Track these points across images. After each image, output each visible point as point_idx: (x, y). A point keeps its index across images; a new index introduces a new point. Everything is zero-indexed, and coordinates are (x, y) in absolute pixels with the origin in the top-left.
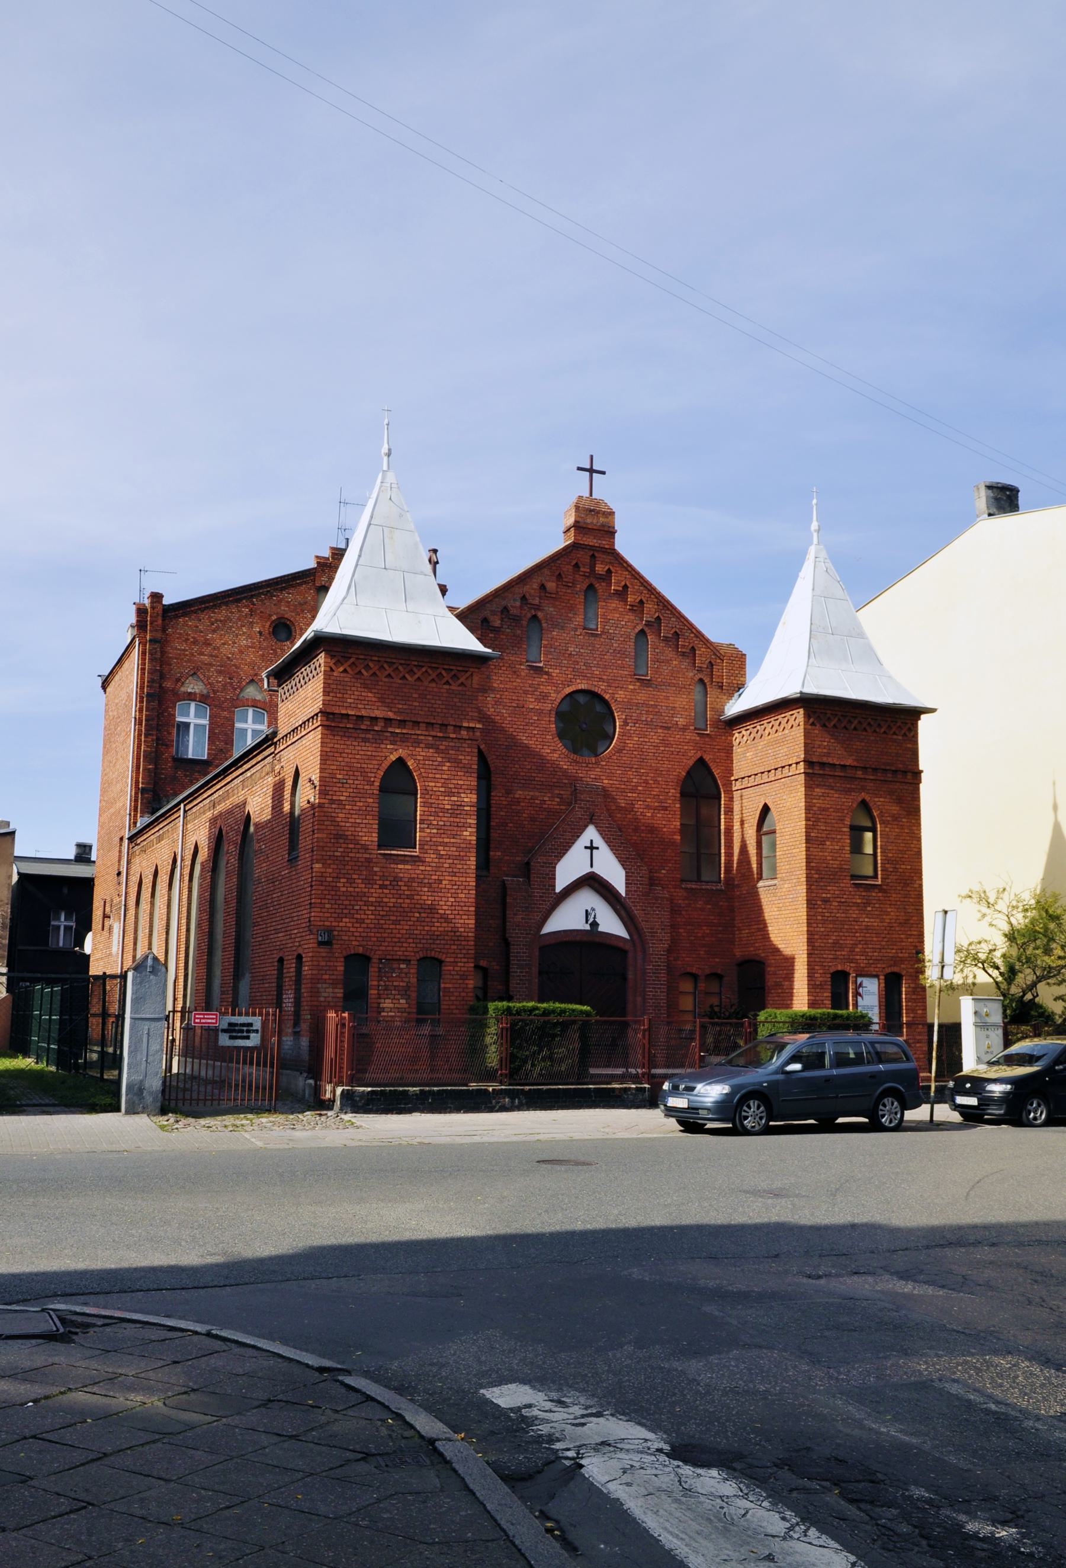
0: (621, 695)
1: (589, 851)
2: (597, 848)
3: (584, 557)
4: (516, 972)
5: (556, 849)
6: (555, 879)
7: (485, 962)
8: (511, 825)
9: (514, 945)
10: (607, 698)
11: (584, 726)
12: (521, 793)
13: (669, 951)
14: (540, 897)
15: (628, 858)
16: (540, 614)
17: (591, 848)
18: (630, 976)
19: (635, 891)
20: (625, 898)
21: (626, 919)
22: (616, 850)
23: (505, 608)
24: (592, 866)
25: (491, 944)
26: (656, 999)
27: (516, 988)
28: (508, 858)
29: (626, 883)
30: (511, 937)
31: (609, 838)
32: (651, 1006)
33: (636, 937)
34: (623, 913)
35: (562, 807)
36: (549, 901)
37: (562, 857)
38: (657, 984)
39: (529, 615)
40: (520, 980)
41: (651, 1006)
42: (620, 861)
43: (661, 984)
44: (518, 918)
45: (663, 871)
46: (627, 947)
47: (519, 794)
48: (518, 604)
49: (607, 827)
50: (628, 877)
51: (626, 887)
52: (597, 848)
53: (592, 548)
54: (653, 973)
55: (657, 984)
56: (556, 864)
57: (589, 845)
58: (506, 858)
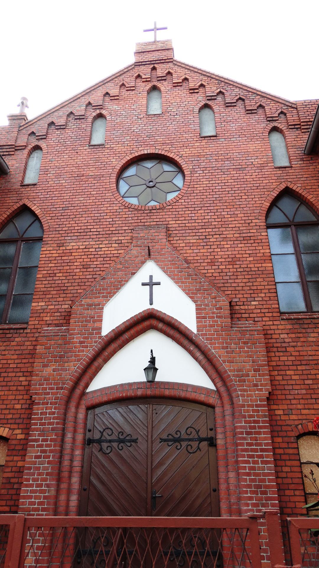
0: (185, 152)
1: (148, 287)
2: (159, 284)
3: (145, 71)
4: (37, 440)
5: (104, 289)
6: (101, 321)
7: (7, 430)
8: (61, 275)
9: (38, 404)
10: (171, 156)
11: (151, 183)
12: (74, 244)
13: (270, 399)
14: (81, 342)
15: (200, 290)
16: (104, 112)
17: (151, 284)
18: (220, 442)
19: (211, 326)
20: (196, 336)
21: (204, 361)
22: (182, 283)
23: (71, 113)
24: (151, 304)
25: (18, 406)
26: (255, 475)
27: (35, 463)
28: (52, 307)
29: (197, 318)
30: (36, 394)
31: (174, 271)
32: (249, 486)
33: (220, 384)
34: (198, 354)
35: (119, 252)
36: (91, 346)
37: (111, 297)
38: (256, 450)
39: (94, 114)
40: (43, 451)
41: (249, 486)
42: (187, 294)
43: (262, 450)
44: (49, 370)
45: (253, 303)
46: (211, 400)
47: (72, 245)
48: (83, 108)
49: (170, 261)
50: (198, 310)
51: (198, 322)
52: (159, 284)
53: (151, 62)
54: (248, 433)
55: (256, 450)
56: (104, 305)
57: (147, 281)
58: (50, 307)
